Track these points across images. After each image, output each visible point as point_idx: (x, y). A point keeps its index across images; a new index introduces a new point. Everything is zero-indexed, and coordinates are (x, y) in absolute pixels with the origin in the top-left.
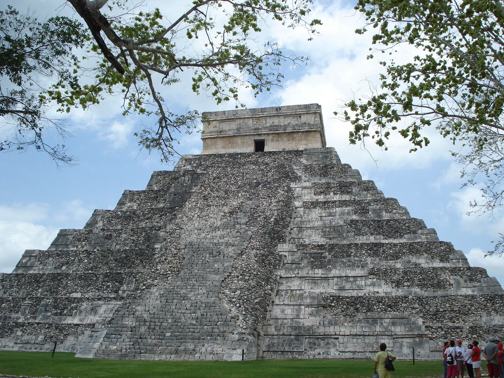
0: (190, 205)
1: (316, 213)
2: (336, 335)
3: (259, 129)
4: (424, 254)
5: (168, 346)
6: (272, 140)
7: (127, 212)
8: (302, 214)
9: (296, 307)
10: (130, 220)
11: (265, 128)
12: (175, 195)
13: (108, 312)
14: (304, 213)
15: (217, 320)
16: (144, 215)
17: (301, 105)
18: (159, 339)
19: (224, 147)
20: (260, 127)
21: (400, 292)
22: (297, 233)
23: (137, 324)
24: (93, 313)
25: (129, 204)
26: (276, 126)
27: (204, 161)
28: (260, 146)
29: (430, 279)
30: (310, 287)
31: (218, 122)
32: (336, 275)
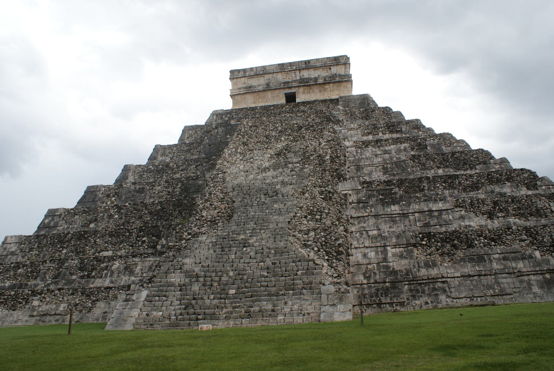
0: (230, 151)
1: (369, 152)
2: (443, 277)
3: (289, 82)
4: (507, 182)
5: (234, 308)
6: (304, 93)
7: (159, 165)
8: (355, 153)
9: (379, 249)
10: (163, 173)
11: (295, 81)
12: (210, 146)
14: (357, 153)
17: (330, 58)
18: (221, 298)
19: (254, 103)
20: (290, 80)
21: (496, 224)
22: (355, 171)
23: (187, 280)
24: (127, 273)
26: (306, 79)
27: (236, 115)
28: (291, 98)
29: (525, 209)
31: (246, 78)
32: (417, 211)
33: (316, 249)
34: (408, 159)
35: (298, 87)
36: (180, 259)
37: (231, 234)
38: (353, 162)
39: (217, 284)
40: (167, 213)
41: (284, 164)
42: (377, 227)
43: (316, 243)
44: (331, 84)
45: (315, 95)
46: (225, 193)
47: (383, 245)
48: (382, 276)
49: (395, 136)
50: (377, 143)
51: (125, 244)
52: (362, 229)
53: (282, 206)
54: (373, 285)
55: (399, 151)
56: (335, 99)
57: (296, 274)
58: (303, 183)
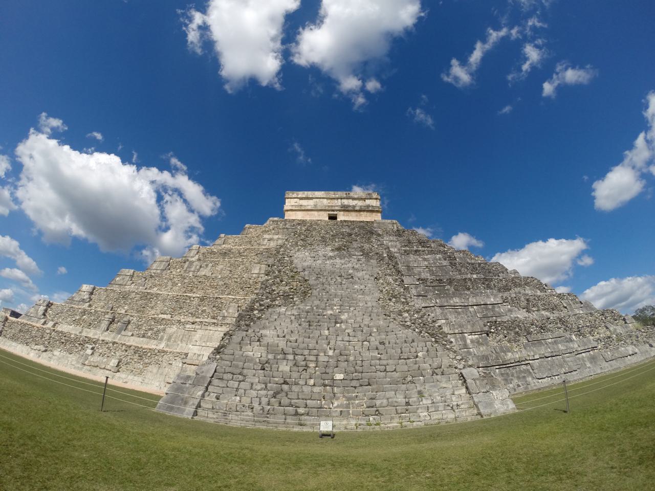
6: (344, 215)
9: (458, 336)
11: (337, 206)
14: (401, 258)
15: (413, 350)
23: (270, 356)
31: (298, 199)
33: (417, 330)
35: (340, 211)
37: (315, 308)
39: (314, 365)
42: (444, 316)
45: (352, 217)
47: (460, 332)
51: (185, 311)
57: (417, 356)
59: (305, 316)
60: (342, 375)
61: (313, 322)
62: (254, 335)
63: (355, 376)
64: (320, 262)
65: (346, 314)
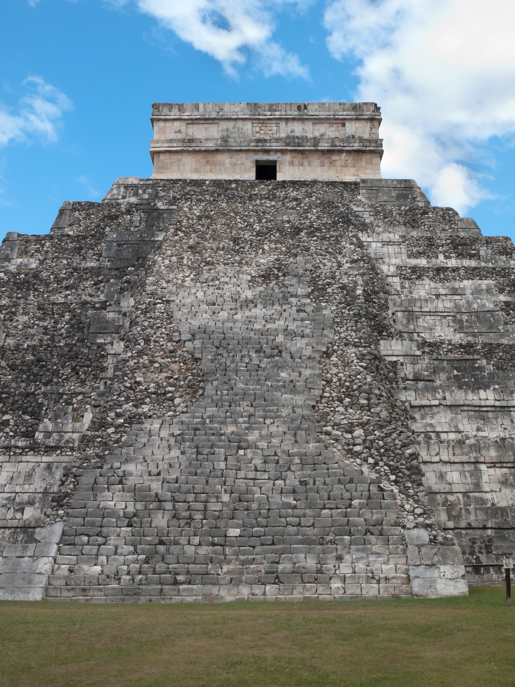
0: (167, 262)
1: (424, 288)
3: (265, 141)
5: (244, 563)
6: (292, 163)
7: (19, 274)
8: (399, 288)
9: (467, 468)
10: (28, 289)
11: (278, 140)
12: (119, 245)
13: (21, 481)
14: (403, 287)
15: (347, 495)
16: (59, 281)
19: (197, 171)
20: (267, 137)
22: (405, 321)
23: (140, 506)
25: (20, 260)
26: (298, 137)
27: (164, 191)
28: (266, 171)
30: (475, 427)
31: (184, 124)
33: (371, 460)
34: (498, 308)
36: (117, 465)
37: (208, 421)
38: (401, 305)
39: (201, 517)
40: (48, 370)
41: (281, 295)
43: (370, 449)
44: (344, 154)
46: (178, 342)
47: (473, 460)
48: (480, 517)
49: (468, 263)
50: (439, 274)
52: (429, 429)
53: (294, 376)
54: (464, 532)
55: (477, 292)
56: (351, 183)
57: (350, 506)
58: (326, 336)
59: (191, 437)
60: (238, 530)
61: (203, 447)
62: (112, 474)
63: (256, 531)
64: (223, 315)
65: (256, 432)
